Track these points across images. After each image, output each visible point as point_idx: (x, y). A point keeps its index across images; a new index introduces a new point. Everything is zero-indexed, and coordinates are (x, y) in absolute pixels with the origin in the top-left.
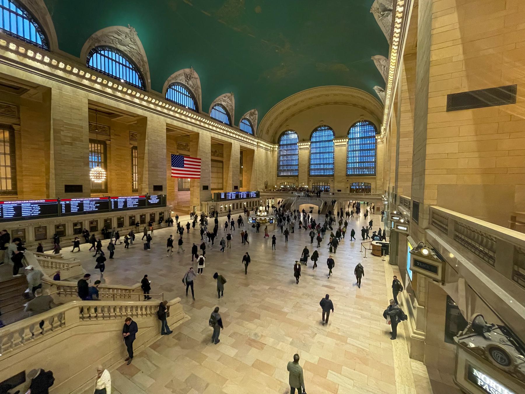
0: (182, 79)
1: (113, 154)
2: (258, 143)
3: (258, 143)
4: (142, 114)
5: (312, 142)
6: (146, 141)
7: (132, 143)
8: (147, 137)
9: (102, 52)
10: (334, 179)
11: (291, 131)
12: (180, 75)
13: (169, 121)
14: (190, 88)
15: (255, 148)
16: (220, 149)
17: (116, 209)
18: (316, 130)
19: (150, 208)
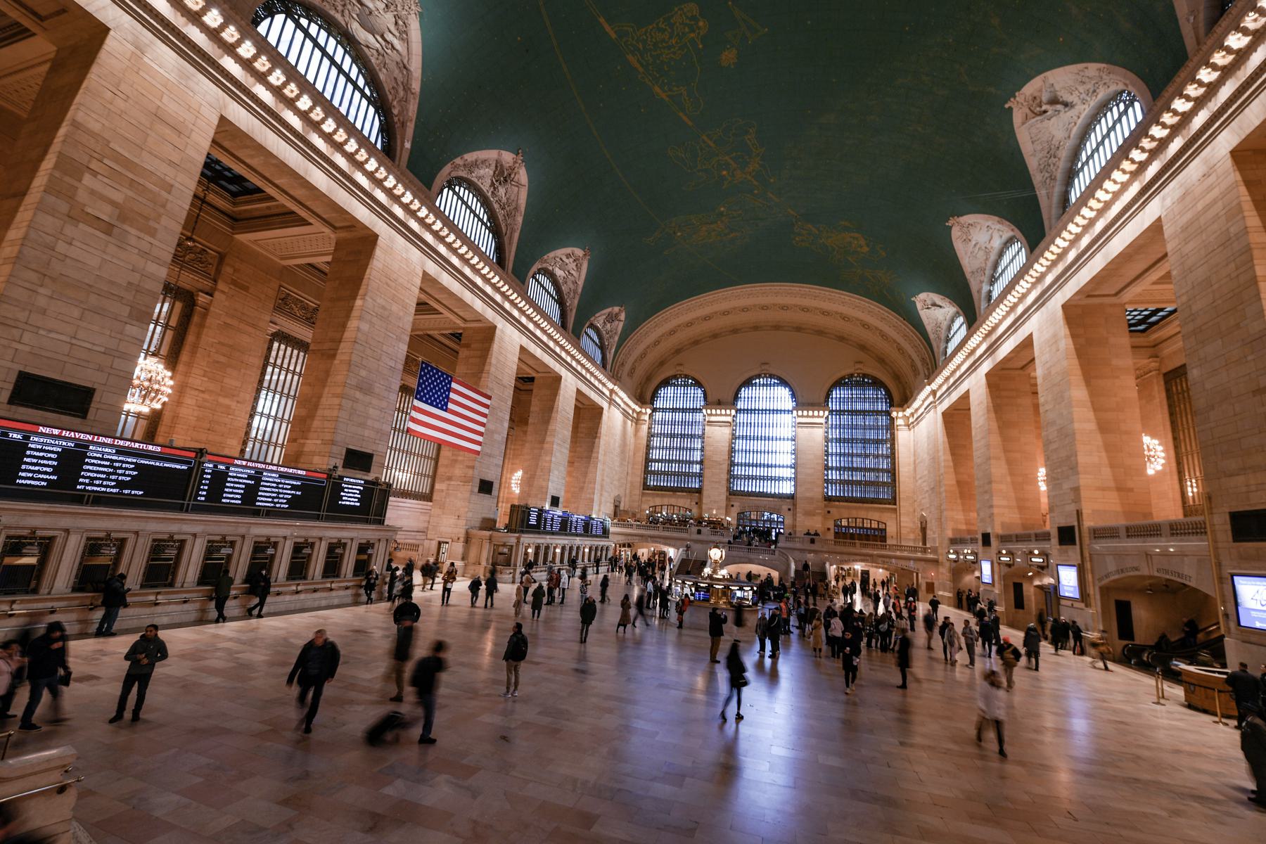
0: (484, 177)
1: (209, 336)
2: (612, 391)
3: (612, 391)
4: (367, 223)
5: (738, 411)
6: (358, 302)
7: (278, 321)
8: (361, 292)
9: (304, 22)
10: (795, 505)
11: (687, 377)
12: (486, 160)
13: (432, 268)
14: (496, 206)
15: (605, 405)
16: (533, 386)
17: (214, 505)
18: (748, 383)
19: (333, 519)
